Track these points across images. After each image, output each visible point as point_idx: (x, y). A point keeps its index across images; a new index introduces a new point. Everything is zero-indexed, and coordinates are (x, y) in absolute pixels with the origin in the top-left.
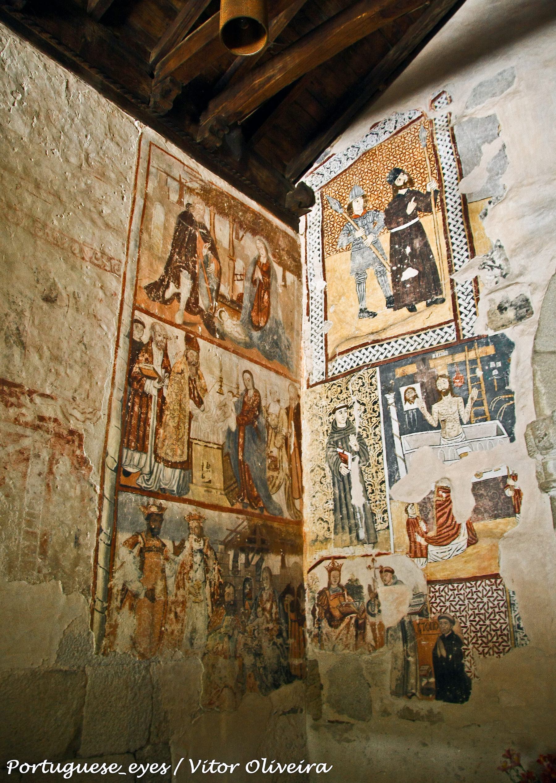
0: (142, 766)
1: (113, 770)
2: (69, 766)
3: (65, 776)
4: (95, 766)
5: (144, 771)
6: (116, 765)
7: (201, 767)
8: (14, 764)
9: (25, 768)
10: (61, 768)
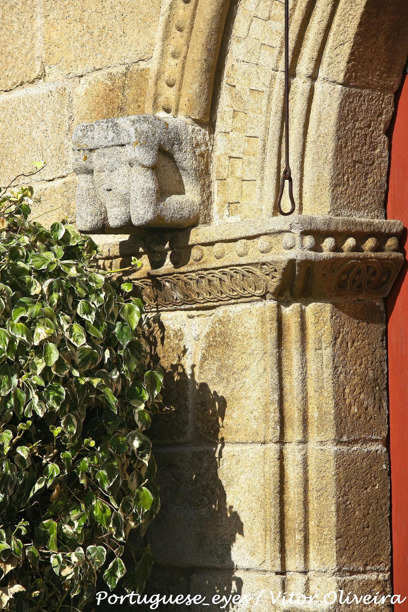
0: (224, 597)
1: (197, 601)
2: (155, 598)
3: (151, 607)
4: (180, 597)
6: (200, 597)
8: (103, 595)
9: (113, 599)
10: (148, 599)
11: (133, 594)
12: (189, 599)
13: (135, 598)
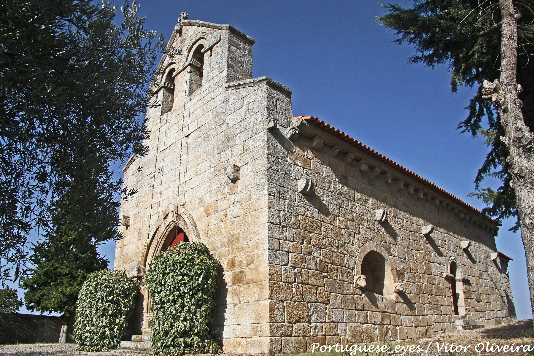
0: (403, 347)
3: (351, 354)
5: (405, 351)
7: (444, 347)
8: (316, 346)
11: (338, 344)
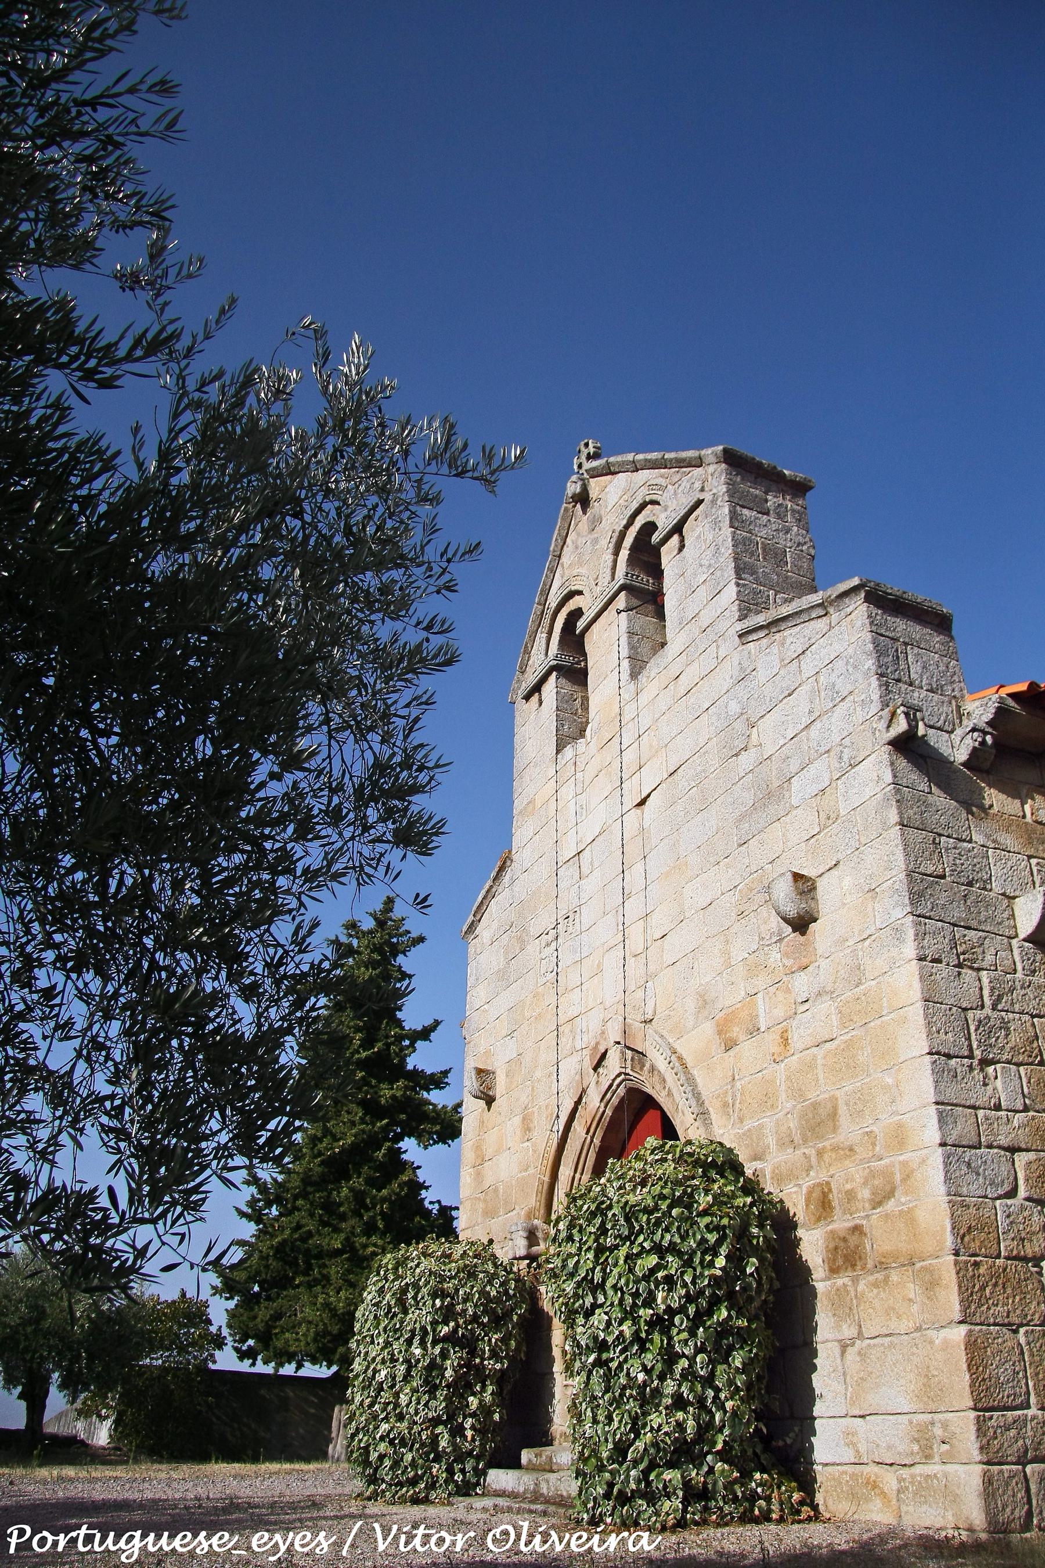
1: (219, 1546)
2: (132, 1537)
3: (123, 1558)
5: (283, 1548)
7: (396, 1538)
11: (84, 1531)
12: (323, 1541)
13: (89, 1539)
